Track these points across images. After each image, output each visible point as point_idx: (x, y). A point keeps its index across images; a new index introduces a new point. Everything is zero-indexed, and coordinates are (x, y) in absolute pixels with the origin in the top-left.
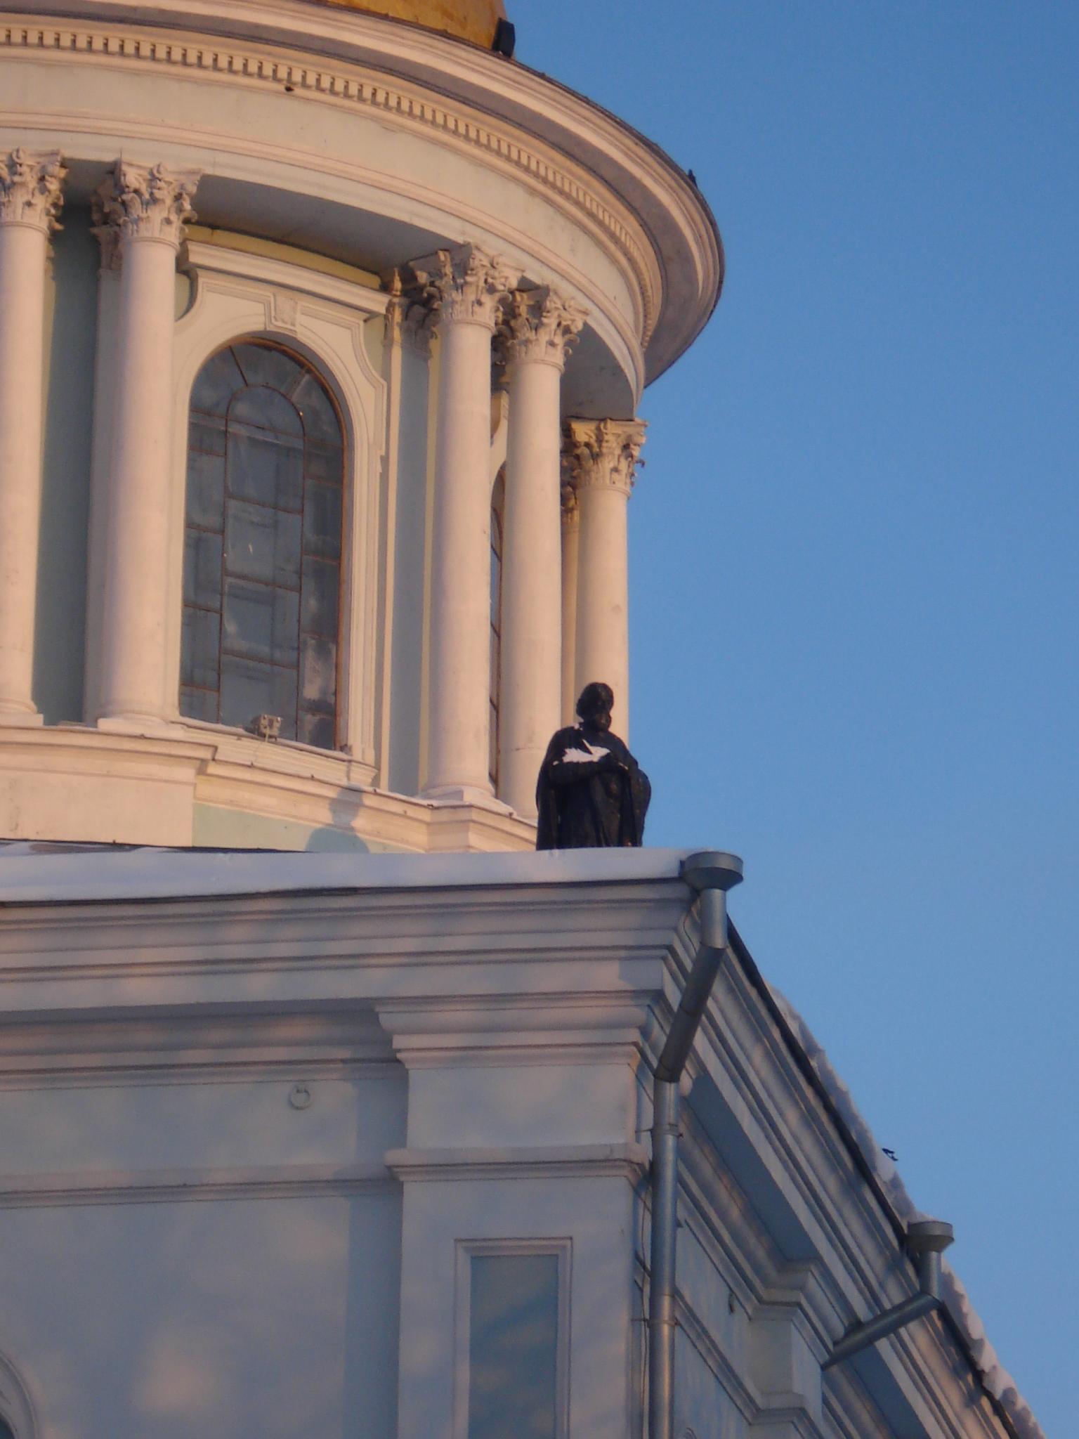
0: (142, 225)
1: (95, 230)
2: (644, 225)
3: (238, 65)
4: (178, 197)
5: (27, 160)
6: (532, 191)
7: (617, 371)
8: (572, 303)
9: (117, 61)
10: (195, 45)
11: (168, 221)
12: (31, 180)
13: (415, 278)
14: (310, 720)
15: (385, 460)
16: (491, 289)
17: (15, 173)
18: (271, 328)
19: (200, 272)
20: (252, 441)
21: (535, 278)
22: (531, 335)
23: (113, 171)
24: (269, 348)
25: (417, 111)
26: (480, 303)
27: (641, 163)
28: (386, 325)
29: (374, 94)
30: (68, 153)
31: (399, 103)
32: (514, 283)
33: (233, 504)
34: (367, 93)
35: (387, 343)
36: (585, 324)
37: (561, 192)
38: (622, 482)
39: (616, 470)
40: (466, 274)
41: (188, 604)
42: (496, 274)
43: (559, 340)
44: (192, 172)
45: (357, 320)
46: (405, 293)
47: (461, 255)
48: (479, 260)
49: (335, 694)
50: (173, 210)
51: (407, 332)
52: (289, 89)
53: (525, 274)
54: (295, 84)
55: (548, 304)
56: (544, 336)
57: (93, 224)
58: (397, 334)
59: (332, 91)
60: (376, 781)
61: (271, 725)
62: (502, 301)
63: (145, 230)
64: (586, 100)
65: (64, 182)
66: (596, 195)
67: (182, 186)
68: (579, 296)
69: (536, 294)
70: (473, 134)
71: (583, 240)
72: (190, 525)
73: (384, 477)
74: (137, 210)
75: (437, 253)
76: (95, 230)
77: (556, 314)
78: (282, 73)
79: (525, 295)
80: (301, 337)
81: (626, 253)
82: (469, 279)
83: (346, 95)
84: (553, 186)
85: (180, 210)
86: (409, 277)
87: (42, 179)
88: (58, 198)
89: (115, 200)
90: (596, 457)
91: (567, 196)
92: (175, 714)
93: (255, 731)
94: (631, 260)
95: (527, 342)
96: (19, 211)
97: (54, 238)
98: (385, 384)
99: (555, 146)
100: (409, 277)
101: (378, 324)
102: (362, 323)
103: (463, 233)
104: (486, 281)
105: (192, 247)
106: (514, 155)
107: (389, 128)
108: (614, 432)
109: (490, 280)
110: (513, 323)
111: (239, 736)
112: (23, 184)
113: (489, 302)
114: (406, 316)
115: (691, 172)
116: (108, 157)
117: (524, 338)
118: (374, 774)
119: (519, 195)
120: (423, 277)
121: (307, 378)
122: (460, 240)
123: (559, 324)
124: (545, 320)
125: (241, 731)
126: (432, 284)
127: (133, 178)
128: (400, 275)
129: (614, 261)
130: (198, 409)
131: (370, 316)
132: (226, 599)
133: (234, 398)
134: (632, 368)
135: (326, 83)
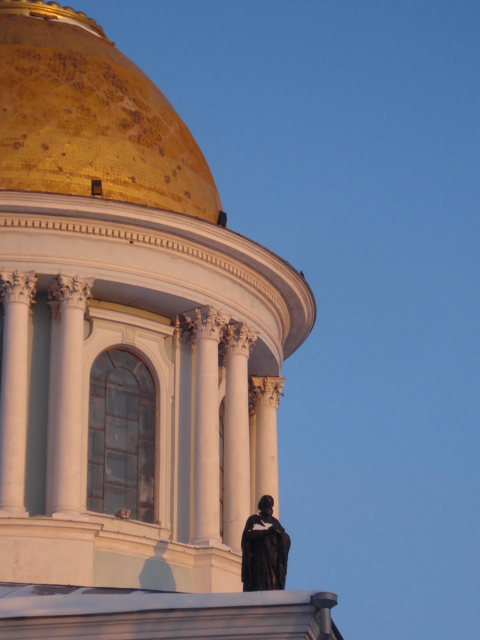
0: (70, 301)
1: (49, 303)
2: (282, 294)
3: (110, 233)
4: (85, 289)
5: (21, 275)
6: (235, 282)
7: (272, 356)
8: (252, 329)
9: (59, 232)
10: (91, 225)
11: (81, 299)
12: (22, 283)
13: (186, 320)
14: (143, 511)
15: (173, 398)
16: (218, 324)
17: (15, 281)
18: (124, 343)
19: (94, 320)
21: (237, 319)
22: (235, 343)
23: (57, 278)
24: (124, 351)
25: (186, 250)
26: (213, 330)
28: (173, 340)
29: (167, 243)
30: (38, 271)
31: (178, 247)
32: (227, 321)
33: (109, 418)
34: (164, 243)
35: (174, 347)
36: (258, 338)
37: (247, 282)
38: (274, 403)
39: (271, 398)
40: (207, 318)
42: (220, 318)
43: (247, 345)
44: (90, 278)
45: (161, 338)
46: (181, 326)
47: (205, 310)
48: (213, 312)
49: (153, 499)
50: (83, 294)
51: (182, 342)
52: (131, 242)
53: (232, 317)
54: (134, 240)
55: (242, 330)
56: (240, 343)
57: (48, 300)
58: (178, 343)
59: (150, 243)
60: (171, 537)
61: (126, 513)
62: (223, 329)
63: (71, 303)
64: (257, 244)
65: (36, 283)
66: (262, 283)
67: (86, 284)
69: (237, 326)
70: (209, 259)
71: (257, 302)
72: (90, 427)
74: (67, 295)
75: (194, 309)
76: (49, 303)
78: (129, 236)
79: (232, 326)
80: (137, 346)
81: (275, 307)
82: (208, 320)
83: (156, 244)
84: (244, 280)
85: (86, 294)
86: (183, 319)
87: (27, 283)
88: (34, 290)
89: (58, 290)
90: (263, 392)
91: (250, 284)
94: (277, 310)
95: (233, 346)
96: (17, 296)
97: (32, 306)
98: (173, 365)
99: (244, 263)
100: (183, 319)
101: (170, 339)
102: (163, 339)
103: (206, 301)
104: (216, 321)
105: (90, 309)
106: (227, 267)
107: (173, 257)
108: (270, 382)
109: (217, 321)
110: (227, 338)
112: (19, 285)
113: (217, 330)
114: (182, 336)
115: (301, 272)
116: (55, 273)
117: (232, 344)
118: (170, 534)
119: (229, 284)
120: (189, 319)
121: (140, 363)
122: (205, 304)
123: (247, 338)
124: (241, 336)
126: (193, 322)
127: (65, 281)
128: (179, 319)
129: (269, 310)
130: (94, 378)
131: (166, 336)
132: (106, 458)
133: (109, 372)
135: (147, 239)
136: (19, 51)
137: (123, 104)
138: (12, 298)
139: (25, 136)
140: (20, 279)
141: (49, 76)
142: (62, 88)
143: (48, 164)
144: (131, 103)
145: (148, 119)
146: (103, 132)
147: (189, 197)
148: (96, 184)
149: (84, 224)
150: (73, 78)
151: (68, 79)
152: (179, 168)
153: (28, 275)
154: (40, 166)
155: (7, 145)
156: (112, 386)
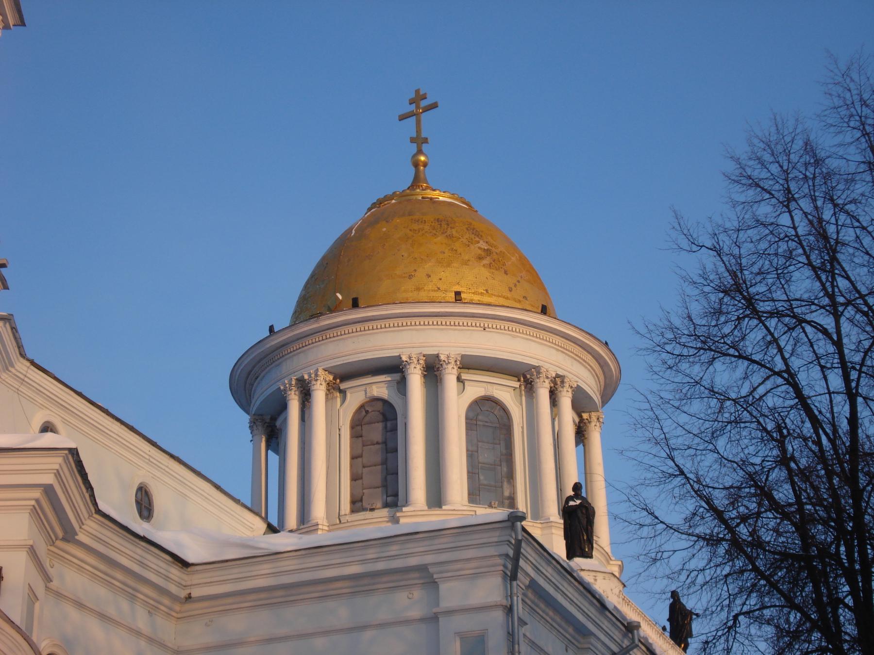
0: (446, 370)
1: (436, 373)
2: (593, 357)
3: (470, 324)
4: (456, 361)
5: (413, 356)
7: (591, 398)
10: (457, 320)
11: (453, 368)
13: (526, 377)
14: (507, 502)
15: (523, 428)
16: (547, 378)
20: (484, 426)
22: (562, 389)
23: (437, 356)
24: (488, 400)
25: (521, 331)
27: (589, 339)
32: (554, 375)
33: (480, 444)
34: (506, 328)
35: (521, 395)
36: (577, 385)
37: (567, 350)
38: (598, 429)
39: (595, 425)
41: (468, 472)
43: (570, 390)
44: (458, 354)
45: (511, 390)
46: (524, 381)
47: (538, 369)
48: (543, 370)
51: (526, 392)
55: (565, 380)
56: (565, 389)
57: (435, 371)
58: (523, 392)
59: (496, 328)
66: (577, 350)
67: (456, 358)
68: (575, 377)
69: (562, 378)
71: (575, 363)
73: (523, 432)
74: (445, 366)
76: (436, 373)
77: (568, 383)
80: (496, 396)
81: (589, 365)
83: (501, 329)
84: (564, 348)
85: (456, 365)
86: (525, 377)
87: (418, 360)
90: (590, 422)
91: (569, 351)
92: (467, 503)
93: (490, 506)
94: (591, 366)
100: (525, 377)
101: (518, 390)
103: (538, 363)
105: (462, 374)
106: (551, 341)
107: (514, 337)
111: (486, 508)
113: (547, 381)
114: (526, 387)
115: (606, 342)
116: (436, 353)
119: (554, 351)
120: (528, 376)
121: (499, 407)
122: (537, 365)
125: (487, 506)
127: (442, 357)
129: (586, 368)
131: (515, 389)
133: (478, 415)
134: (597, 398)
135: (494, 327)
136: (412, 219)
137: (479, 245)
138: (409, 371)
139: (415, 270)
140: (413, 358)
141: (430, 233)
142: (439, 238)
143: (430, 287)
144: (484, 244)
145: (496, 253)
146: (466, 263)
147: (526, 299)
148: (458, 294)
149: (452, 320)
150: (446, 232)
151: (443, 233)
152: (519, 282)
153: (418, 355)
154: (425, 288)
155: (404, 277)
156: (481, 423)
